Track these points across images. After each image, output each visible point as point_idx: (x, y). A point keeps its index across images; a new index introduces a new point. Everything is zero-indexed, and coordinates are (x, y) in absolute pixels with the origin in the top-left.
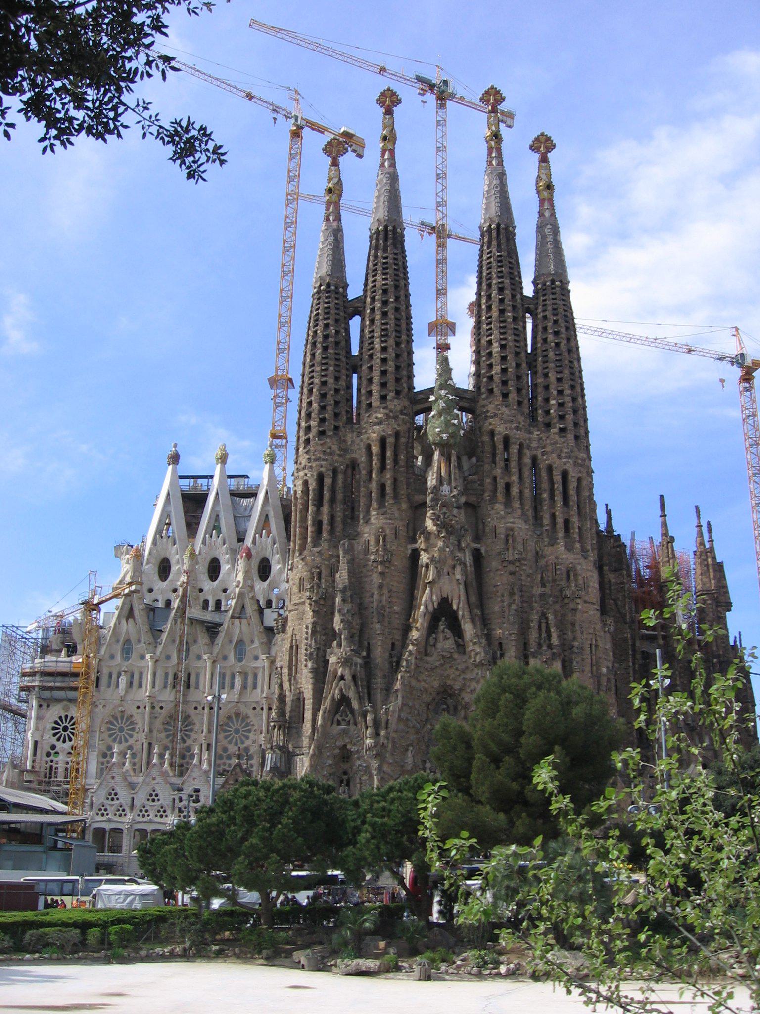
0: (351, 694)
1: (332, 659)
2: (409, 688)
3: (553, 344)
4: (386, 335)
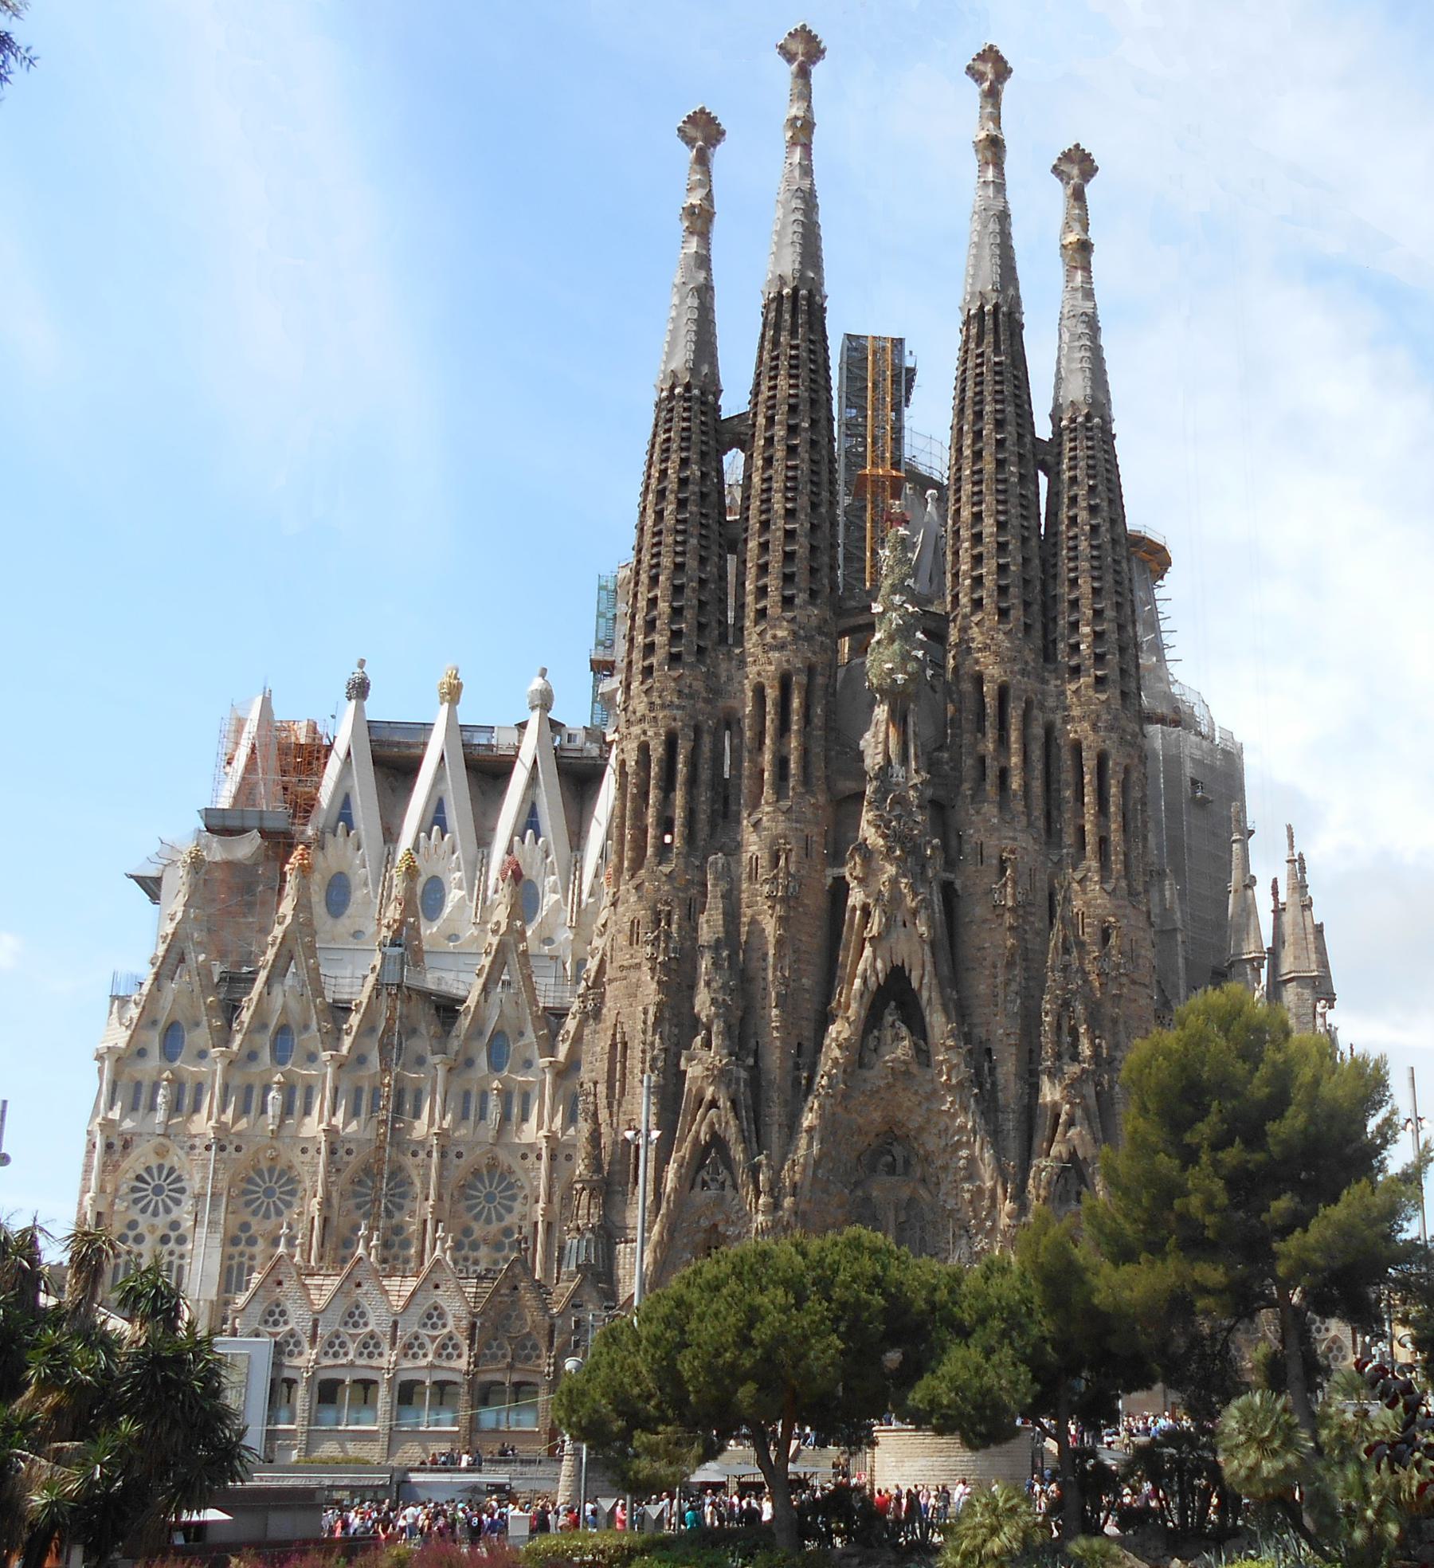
0: (731, 1133)
1: (693, 1071)
2: (829, 1127)
3: (1087, 528)
4: (794, 489)
